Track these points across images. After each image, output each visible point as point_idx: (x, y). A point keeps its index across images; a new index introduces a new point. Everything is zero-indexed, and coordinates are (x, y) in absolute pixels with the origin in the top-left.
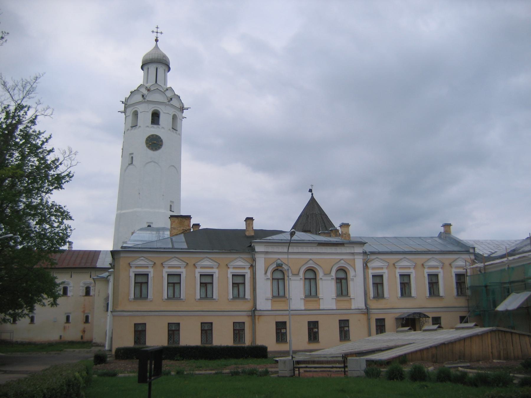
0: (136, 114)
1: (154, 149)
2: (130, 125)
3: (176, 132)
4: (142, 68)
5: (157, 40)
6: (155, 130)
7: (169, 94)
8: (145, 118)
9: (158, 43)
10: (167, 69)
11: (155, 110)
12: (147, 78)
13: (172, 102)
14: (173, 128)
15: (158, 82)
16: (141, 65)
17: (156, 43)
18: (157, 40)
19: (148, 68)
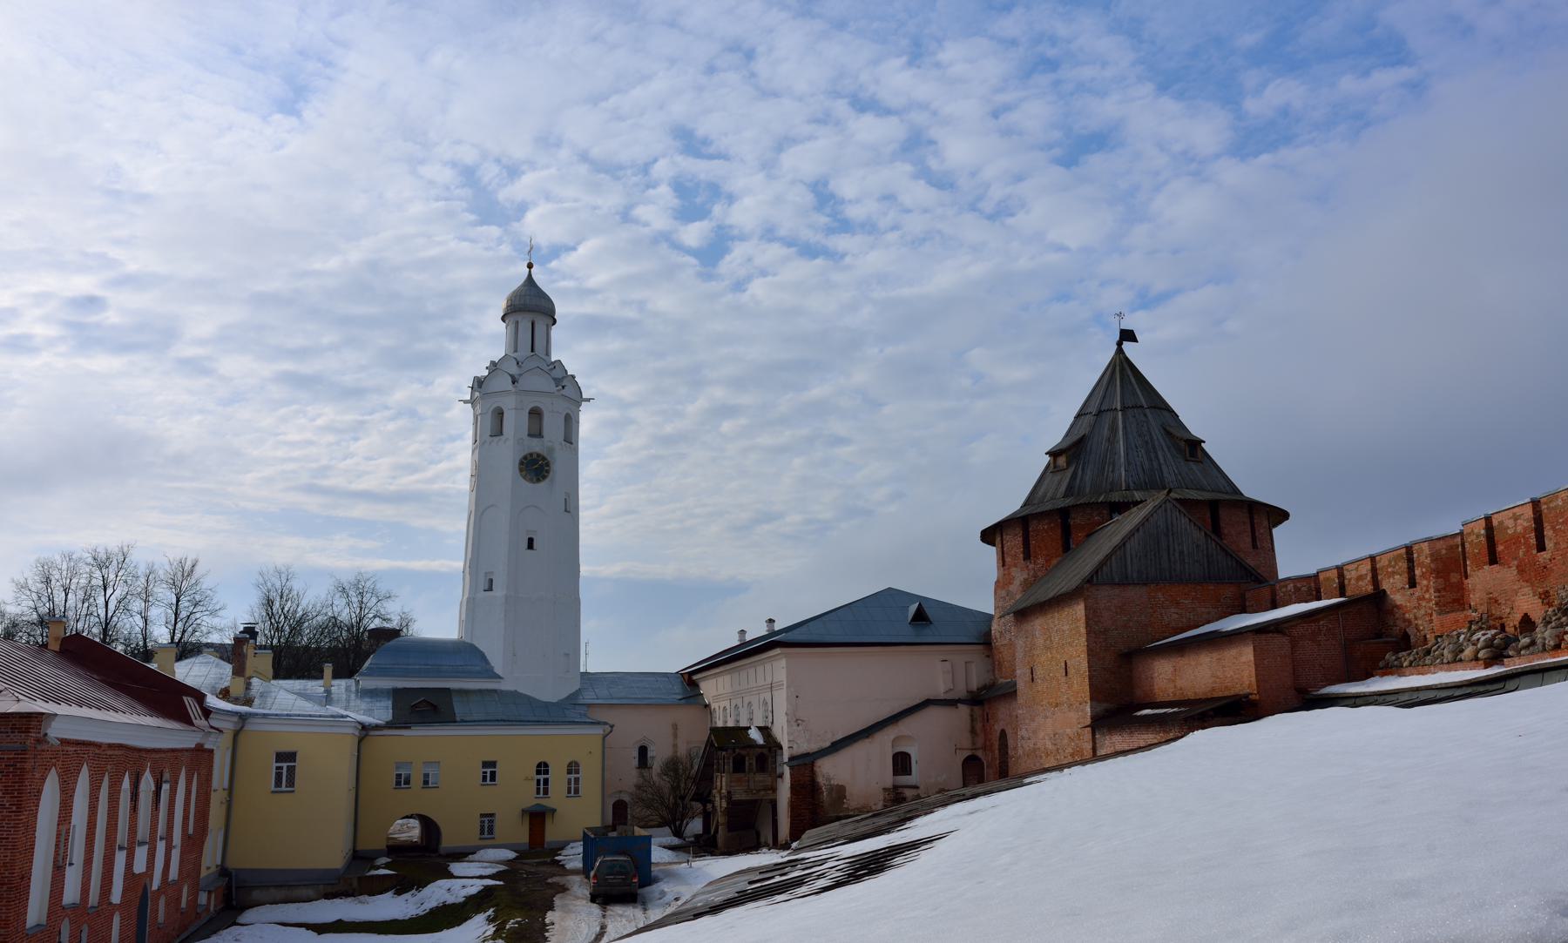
0: (499, 414)
1: (535, 480)
2: (489, 433)
3: (570, 448)
4: (503, 319)
5: (530, 266)
6: (536, 446)
7: (557, 373)
8: (515, 423)
9: (532, 270)
10: (551, 321)
11: (536, 407)
12: (515, 343)
13: (563, 392)
14: (565, 440)
15: (536, 348)
16: (502, 314)
17: (530, 272)
18: (530, 266)
19: (517, 322)
